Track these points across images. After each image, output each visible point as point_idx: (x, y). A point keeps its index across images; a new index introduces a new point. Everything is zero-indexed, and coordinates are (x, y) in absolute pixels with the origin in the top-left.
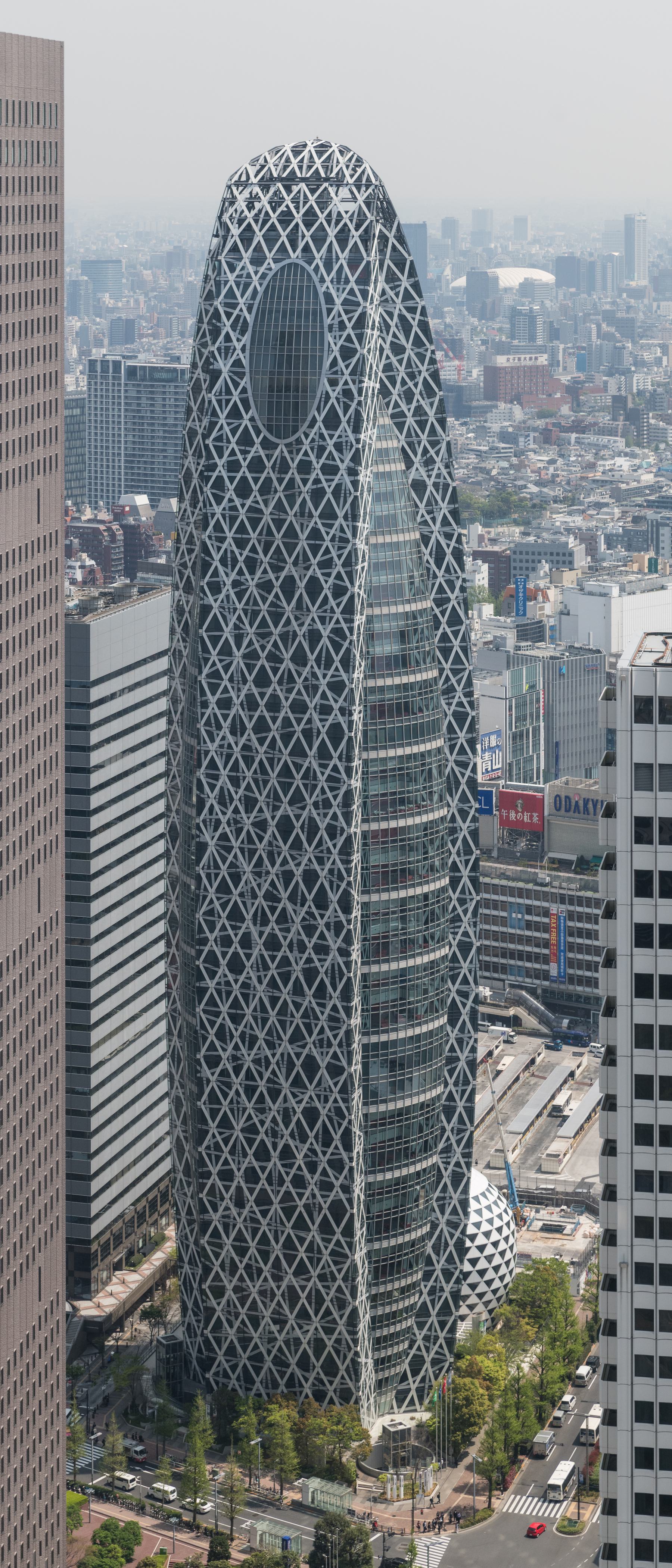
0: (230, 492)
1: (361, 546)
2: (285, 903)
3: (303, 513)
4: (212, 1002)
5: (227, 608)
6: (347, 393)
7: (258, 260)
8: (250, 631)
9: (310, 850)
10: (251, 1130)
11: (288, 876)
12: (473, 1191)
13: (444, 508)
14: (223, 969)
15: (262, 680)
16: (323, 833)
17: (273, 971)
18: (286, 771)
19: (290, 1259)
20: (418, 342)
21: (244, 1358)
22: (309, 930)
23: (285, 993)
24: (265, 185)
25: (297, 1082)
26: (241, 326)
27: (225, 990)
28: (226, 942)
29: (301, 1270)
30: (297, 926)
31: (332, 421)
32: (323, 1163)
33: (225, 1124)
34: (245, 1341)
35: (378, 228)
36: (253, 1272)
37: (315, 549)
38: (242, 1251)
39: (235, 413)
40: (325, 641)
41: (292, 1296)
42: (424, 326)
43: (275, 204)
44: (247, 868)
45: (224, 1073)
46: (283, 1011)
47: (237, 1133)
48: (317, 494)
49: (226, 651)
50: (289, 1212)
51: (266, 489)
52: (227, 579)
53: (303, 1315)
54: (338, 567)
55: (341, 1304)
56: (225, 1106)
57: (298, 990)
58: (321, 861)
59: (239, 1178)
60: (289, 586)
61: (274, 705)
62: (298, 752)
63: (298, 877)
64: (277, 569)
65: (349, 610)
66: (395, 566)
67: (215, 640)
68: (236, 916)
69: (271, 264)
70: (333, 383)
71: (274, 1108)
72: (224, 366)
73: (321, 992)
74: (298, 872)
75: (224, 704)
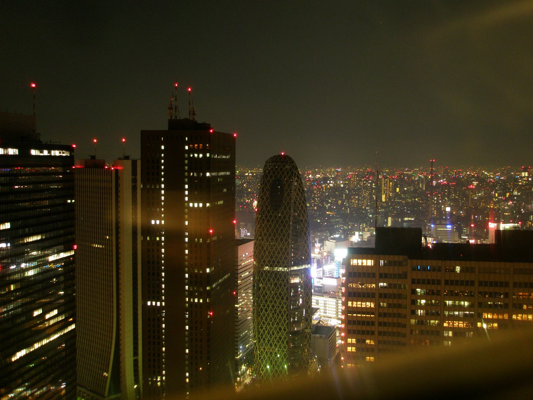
1: (291, 232)
2: (275, 299)
4: (262, 317)
6: (288, 203)
7: (271, 177)
9: (280, 290)
10: (269, 341)
11: (276, 294)
12: (311, 352)
14: (264, 311)
15: (272, 257)
16: (283, 286)
17: (273, 311)
19: (276, 365)
20: (302, 193)
22: (280, 304)
23: (275, 316)
25: (278, 332)
27: (264, 315)
30: (278, 303)
33: (264, 339)
35: (294, 171)
37: (282, 232)
40: (283, 250)
45: (264, 330)
46: (275, 319)
47: (266, 341)
49: (265, 251)
51: (273, 221)
56: (264, 336)
57: (278, 315)
58: (282, 291)
63: (278, 294)
64: (274, 236)
67: (262, 250)
70: (286, 201)
73: (282, 315)
74: (278, 293)
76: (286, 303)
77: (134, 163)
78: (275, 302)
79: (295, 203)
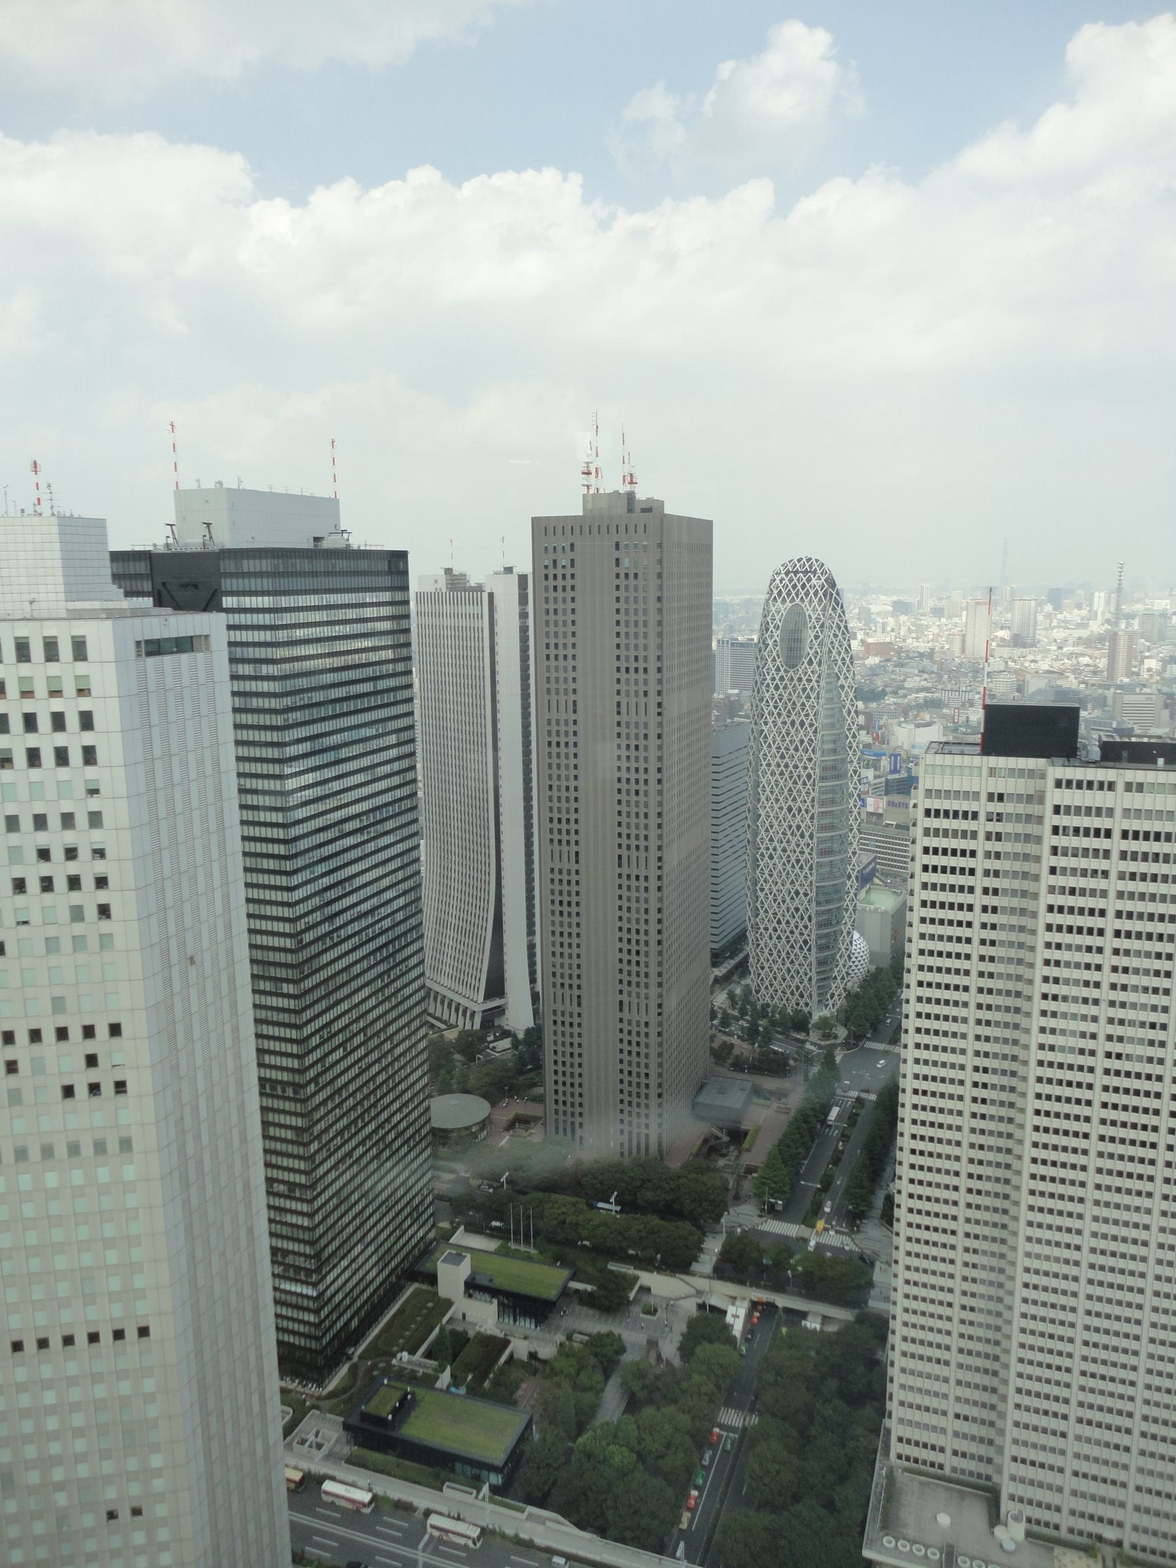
5: (770, 731)
7: (784, 601)
8: (778, 739)
9: (798, 818)
13: (851, 695)
15: (783, 757)
21: (771, 990)
23: (789, 867)
24: (787, 573)
31: (810, 662)
39: (774, 660)
41: (789, 971)
43: (791, 580)
44: (776, 823)
48: (804, 690)
51: (785, 688)
52: (770, 720)
60: (793, 723)
61: (787, 766)
62: (795, 783)
65: (815, 732)
68: (771, 840)
69: (788, 604)
71: (784, 907)
72: (770, 642)
73: (801, 868)
75: (769, 765)
77: (523, 579)
79: (830, 652)
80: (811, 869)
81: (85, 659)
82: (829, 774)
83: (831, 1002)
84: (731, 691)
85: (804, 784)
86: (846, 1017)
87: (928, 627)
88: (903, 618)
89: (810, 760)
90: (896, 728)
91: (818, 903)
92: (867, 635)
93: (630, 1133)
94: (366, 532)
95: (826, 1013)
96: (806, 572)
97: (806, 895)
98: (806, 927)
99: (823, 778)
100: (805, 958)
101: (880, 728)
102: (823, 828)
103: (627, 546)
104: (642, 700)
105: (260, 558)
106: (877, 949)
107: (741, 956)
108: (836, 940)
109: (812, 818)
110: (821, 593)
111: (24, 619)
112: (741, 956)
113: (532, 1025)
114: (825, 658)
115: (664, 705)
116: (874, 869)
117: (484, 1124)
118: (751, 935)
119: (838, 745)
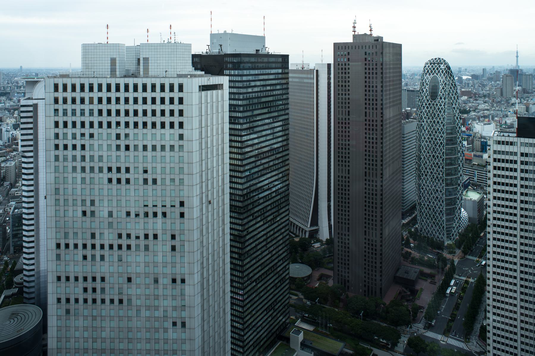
0: (426, 108)
3: (437, 111)
5: (425, 125)
7: (430, 74)
8: (428, 128)
10: (428, 199)
11: (434, 163)
13: (458, 111)
15: (430, 135)
18: (434, 148)
22: (437, 171)
23: (433, 180)
24: (431, 64)
25: (435, 193)
26: (427, 84)
27: (424, 179)
28: (425, 172)
29: (435, 219)
31: (441, 98)
32: (439, 204)
33: (424, 198)
34: (427, 228)
36: (428, 219)
38: (427, 216)
41: (434, 223)
42: (455, 85)
43: (432, 67)
44: (428, 162)
48: (439, 109)
49: (425, 131)
50: (434, 211)
51: (431, 108)
52: (425, 120)
53: (436, 226)
54: (442, 119)
55: (441, 225)
57: (435, 180)
59: (426, 205)
60: (434, 122)
61: (432, 139)
66: (451, 119)
68: (426, 168)
72: (425, 90)
73: (439, 180)
75: (425, 138)
76: (442, 171)
78: (433, 169)
79: (449, 94)
80: (443, 181)
81: (182, 91)
82: (449, 142)
83: (452, 238)
84: (407, 109)
85: (439, 146)
86: (458, 244)
87: (486, 85)
88: (476, 81)
89: (442, 137)
90: (476, 125)
91: (446, 196)
92: (462, 88)
93: (368, 286)
94: (273, 47)
95: (450, 242)
96: (438, 64)
97: (441, 192)
98: (441, 205)
99: (447, 144)
100: (441, 218)
101: (469, 125)
102: (447, 165)
103: (369, 54)
104: (375, 111)
105: (236, 57)
106: (471, 216)
107: (414, 215)
108: (454, 211)
109: (443, 160)
110: (444, 72)
111: (163, 77)
112: (414, 215)
113: (329, 238)
114: (447, 96)
115: (384, 113)
116: (469, 182)
117: (309, 277)
118: (418, 207)
119: (453, 131)
